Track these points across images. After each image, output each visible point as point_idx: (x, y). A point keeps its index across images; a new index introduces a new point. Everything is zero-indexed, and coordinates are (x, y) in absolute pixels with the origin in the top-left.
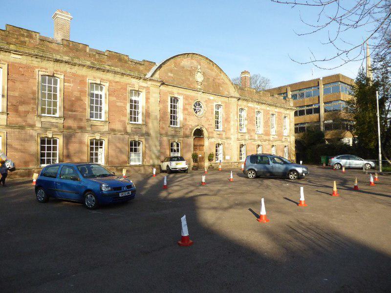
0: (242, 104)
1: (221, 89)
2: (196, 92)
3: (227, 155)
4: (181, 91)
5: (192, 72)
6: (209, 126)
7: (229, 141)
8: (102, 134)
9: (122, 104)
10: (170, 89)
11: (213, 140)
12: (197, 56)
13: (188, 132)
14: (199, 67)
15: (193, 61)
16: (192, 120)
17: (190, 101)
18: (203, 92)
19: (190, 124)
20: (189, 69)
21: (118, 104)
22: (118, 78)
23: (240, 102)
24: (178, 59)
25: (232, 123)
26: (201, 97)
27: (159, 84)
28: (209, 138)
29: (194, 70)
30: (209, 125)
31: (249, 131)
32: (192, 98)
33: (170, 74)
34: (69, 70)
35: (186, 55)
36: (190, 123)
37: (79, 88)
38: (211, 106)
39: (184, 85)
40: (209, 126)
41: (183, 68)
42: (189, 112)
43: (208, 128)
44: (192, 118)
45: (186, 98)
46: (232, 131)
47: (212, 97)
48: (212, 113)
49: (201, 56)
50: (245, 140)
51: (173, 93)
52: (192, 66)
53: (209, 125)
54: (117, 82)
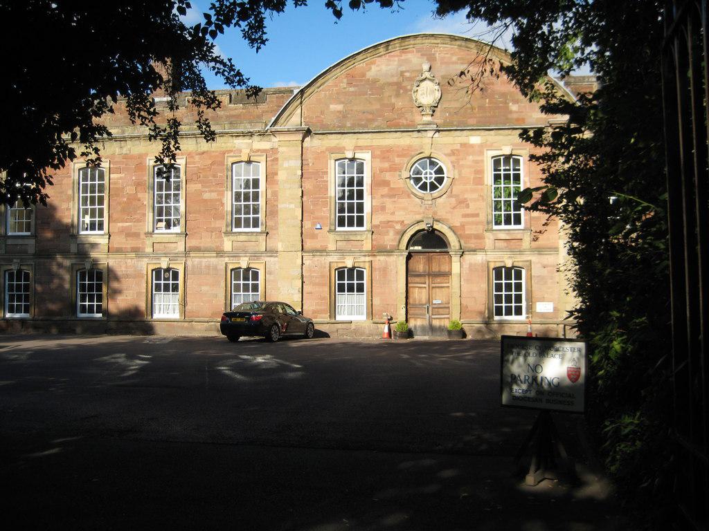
2: (416, 134)
3: (542, 300)
4: (365, 140)
5: (403, 85)
6: (463, 220)
8: (174, 257)
9: (214, 195)
10: (333, 141)
11: (479, 258)
12: (419, 41)
13: (389, 239)
15: (409, 56)
16: (404, 209)
17: (397, 160)
18: (439, 131)
19: (397, 219)
20: (395, 79)
21: (206, 196)
24: (360, 65)
26: (440, 146)
27: (300, 137)
29: (410, 79)
30: (465, 216)
32: (404, 152)
33: (333, 107)
34: (118, 151)
35: (382, 50)
36: (400, 215)
37: (134, 178)
38: (477, 162)
39: (379, 123)
40: (463, 220)
41: (375, 81)
43: (463, 226)
44: (404, 201)
47: (475, 139)
48: (479, 181)
49: (433, 35)
51: (341, 150)
52: (403, 68)
53: (465, 216)
54: (203, 153)
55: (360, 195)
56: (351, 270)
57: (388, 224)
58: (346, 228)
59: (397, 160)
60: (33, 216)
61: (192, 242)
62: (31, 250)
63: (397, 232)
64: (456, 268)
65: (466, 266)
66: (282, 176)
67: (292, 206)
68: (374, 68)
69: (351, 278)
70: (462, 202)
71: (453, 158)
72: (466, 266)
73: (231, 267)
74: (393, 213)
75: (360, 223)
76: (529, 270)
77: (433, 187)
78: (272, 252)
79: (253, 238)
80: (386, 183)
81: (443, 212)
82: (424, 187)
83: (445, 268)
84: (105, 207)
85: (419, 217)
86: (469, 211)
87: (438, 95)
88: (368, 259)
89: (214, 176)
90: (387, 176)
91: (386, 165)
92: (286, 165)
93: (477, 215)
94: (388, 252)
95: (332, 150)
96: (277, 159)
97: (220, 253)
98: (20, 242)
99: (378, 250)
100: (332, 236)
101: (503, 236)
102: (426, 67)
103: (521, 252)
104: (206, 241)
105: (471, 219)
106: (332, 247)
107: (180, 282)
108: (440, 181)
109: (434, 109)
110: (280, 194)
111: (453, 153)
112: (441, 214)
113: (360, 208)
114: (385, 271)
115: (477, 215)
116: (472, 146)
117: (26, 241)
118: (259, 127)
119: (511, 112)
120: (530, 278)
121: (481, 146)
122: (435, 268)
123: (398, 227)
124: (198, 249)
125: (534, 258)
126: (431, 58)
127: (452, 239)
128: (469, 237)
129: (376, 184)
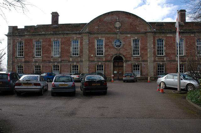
0: (161, 36)
1: (138, 28)
7: (146, 63)
8: (58, 62)
9: (67, 48)
10: (95, 36)
11: (130, 63)
13: (109, 58)
14: (117, 19)
17: (111, 40)
20: (110, 21)
21: (66, 48)
22: (66, 36)
23: (157, 35)
25: (148, 50)
28: (126, 61)
30: (127, 53)
31: (167, 55)
34: (44, 37)
36: (112, 53)
38: (129, 40)
42: (109, 47)
45: (107, 39)
46: (149, 55)
47: (129, 35)
48: (130, 45)
50: (163, 61)
52: (112, 19)
53: (127, 53)
55: (102, 48)
56: (100, 66)
59: (111, 40)
60: (24, 53)
61: (63, 59)
62: (23, 61)
63: (111, 57)
64: (124, 65)
65: (127, 64)
66: (84, 43)
67: (86, 50)
68: (105, 19)
69: (100, 67)
70: (126, 50)
72: (127, 64)
73: (72, 65)
75: (102, 55)
77: (119, 46)
78: (82, 61)
79: (77, 58)
80: (108, 45)
84: (41, 50)
85: (116, 53)
87: (120, 25)
89: (68, 43)
90: (109, 44)
91: (109, 41)
92: (85, 41)
93: (129, 53)
94: (109, 61)
95: (96, 38)
96: (83, 39)
97: (69, 62)
98: (20, 59)
99: (106, 61)
101: (135, 58)
102: (117, 19)
103: (139, 61)
104: (66, 58)
106: (96, 60)
107: (59, 68)
109: (119, 28)
110: (83, 47)
113: (102, 51)
114: (108, 65)
115: (129, 53)
116: (128, 37)
117: (22, 59)
118: (78, 32)
121: (130, 37)
123: (111, 55)
124: (64, 61)
125: (142, 63)
126: (119, 17)
127: (123, 58)
129: (106, 45)
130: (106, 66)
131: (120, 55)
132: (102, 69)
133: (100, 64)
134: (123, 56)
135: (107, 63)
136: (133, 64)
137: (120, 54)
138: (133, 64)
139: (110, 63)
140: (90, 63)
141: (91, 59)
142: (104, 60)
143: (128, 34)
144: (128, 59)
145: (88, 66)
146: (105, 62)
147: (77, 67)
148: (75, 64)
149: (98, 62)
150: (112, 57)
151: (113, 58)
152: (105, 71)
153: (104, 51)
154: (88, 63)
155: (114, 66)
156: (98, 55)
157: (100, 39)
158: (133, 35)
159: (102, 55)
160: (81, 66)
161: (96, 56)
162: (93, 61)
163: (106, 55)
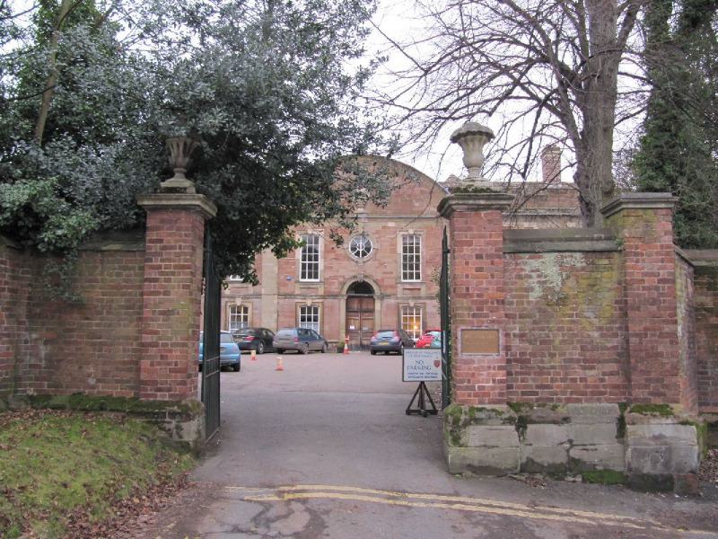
11: (392, 301)
13: (335, 288)
28: (382, 297)
36: (342, 272)
40: (384, 276)
42: (337, 255)
43: (383, 280)
47: (391, 224)
48: (394, 251)
56: (309, 308)
57: (335, 277)
58: (307, 280)
64: (378, 306)
71: (377, 236)
72: (384, 305)
73: (229, 304)
74: (338, 271)
76: (425, 309)
77: (364, 254)
78: (258, 296)
81: (370, 270)
82: (358, 254)
83: (370, 307)
85: (354, 274)
86: (385, 270)
88: (320, 301)
94: (335, 296)
100: (298, 286)
101: (408, 287)
103: (420, 298)
105: (388, 275)
108: (368, 249)
111: (377, 232)
112: (369, 272)
114: (332, 308)
115: (392, 273)
119: (415, 207)
120: (425, 314)
122: (364, 307)
123: (341, 279)
125: (428, 302)
127: (375, 287)
128: (386, 287)
130: (326, 310)
131: (366, 280)
132: (316, 320)
133: (309, 303)
134: (375, 281)
135: (329, 302)
136: (401, 305)
137: (366, 277)
138: (401, 305)
139: (336, 301)
140: (281, 301)
141: (283, 290)
142: (321, 291)
143: (391, 219)
144: (389, 291)
145: (274, 309)
146: (324, 297)
147: (246, 310)
148: (238, 302)
149: (304, 296)
150: (344, 283)
151: (346, 287)
152: (323, 323)
153: (321, 267)
154: (276, 301)
155: (348, 310)
156: (304, 277)
157: (310, 232)
158: (403, 224)
159: (316, 277)
160: (256, 309)
161: (298, 282)
162: (291, 295)
163: (325, 279)
